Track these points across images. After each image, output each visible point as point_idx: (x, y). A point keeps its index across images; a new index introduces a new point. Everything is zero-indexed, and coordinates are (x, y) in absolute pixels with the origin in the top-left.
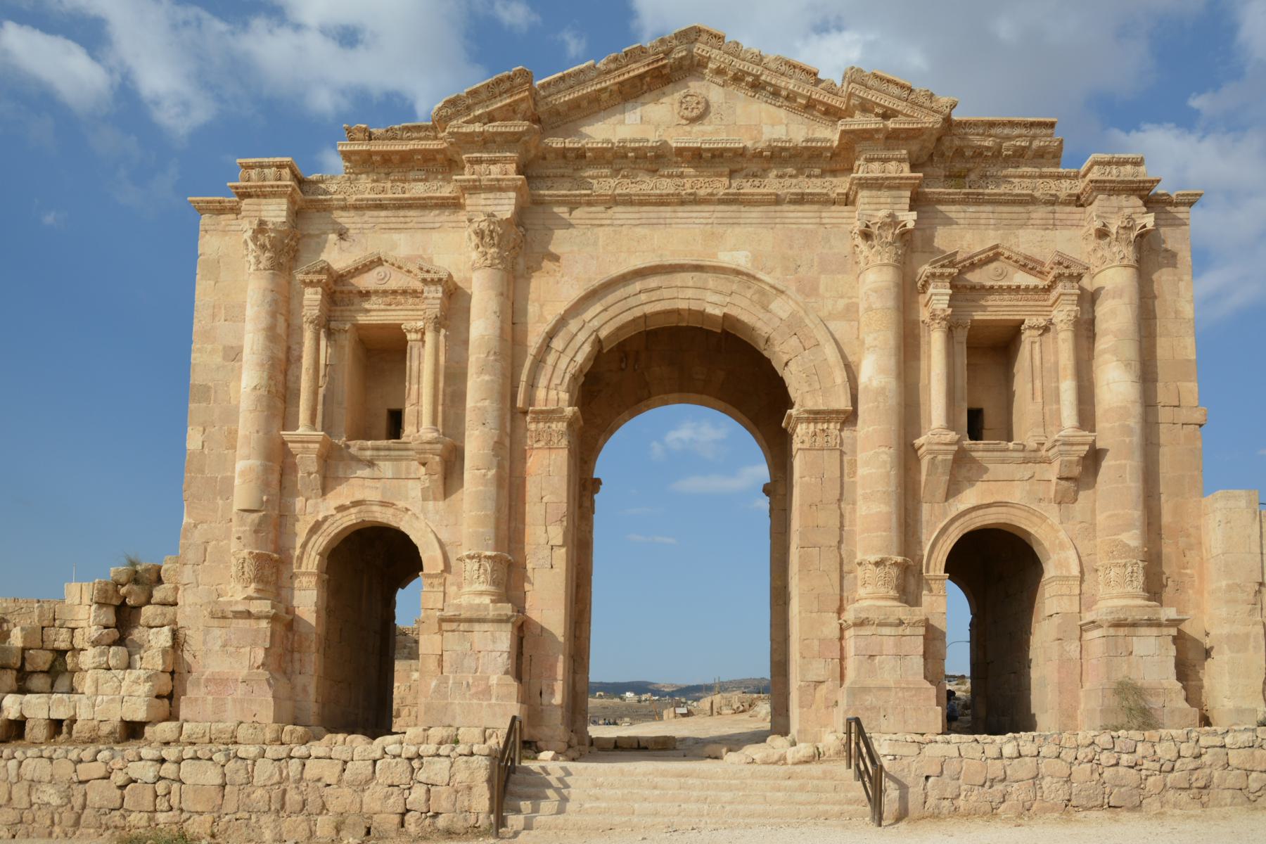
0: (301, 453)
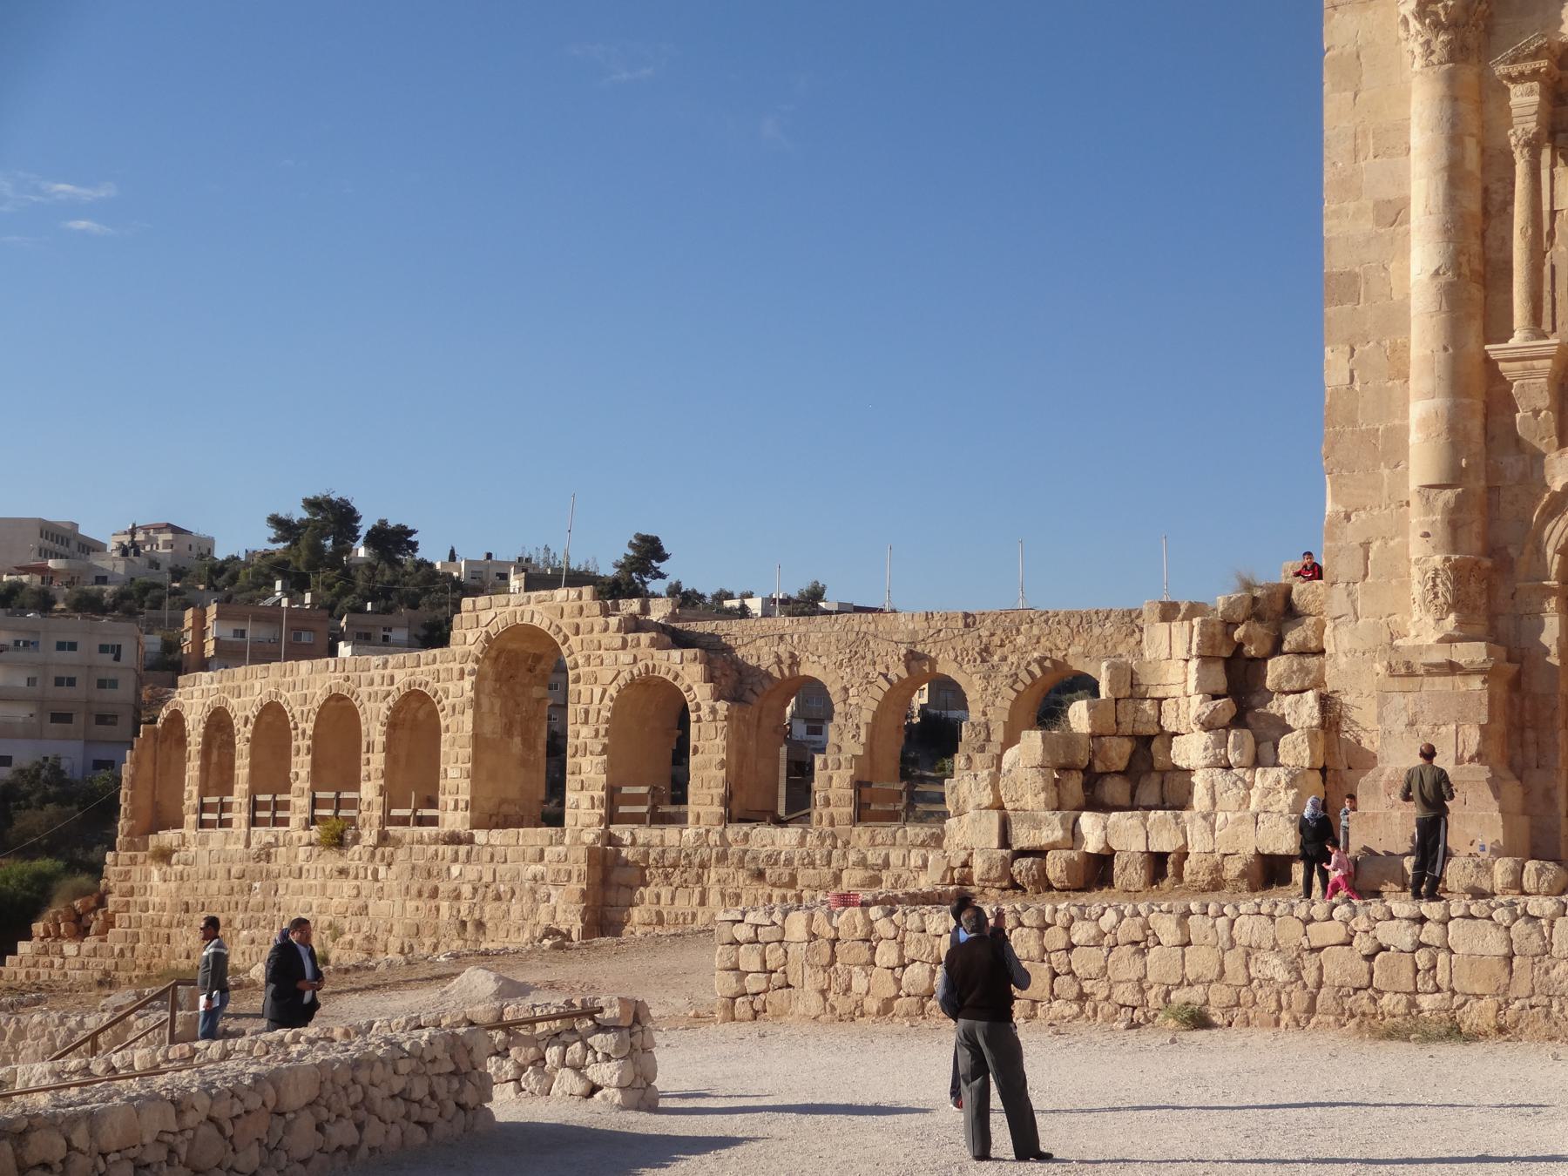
0: (1522, 377)
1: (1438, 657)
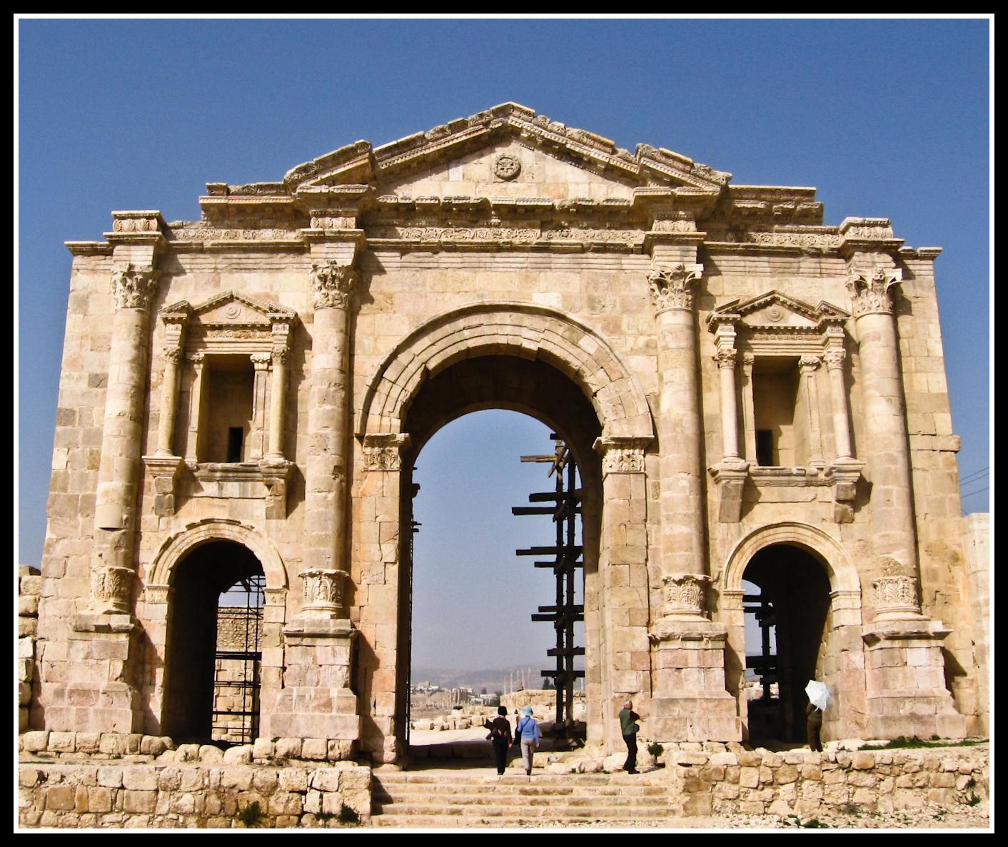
0: (159, 475)
1: (102, 622)
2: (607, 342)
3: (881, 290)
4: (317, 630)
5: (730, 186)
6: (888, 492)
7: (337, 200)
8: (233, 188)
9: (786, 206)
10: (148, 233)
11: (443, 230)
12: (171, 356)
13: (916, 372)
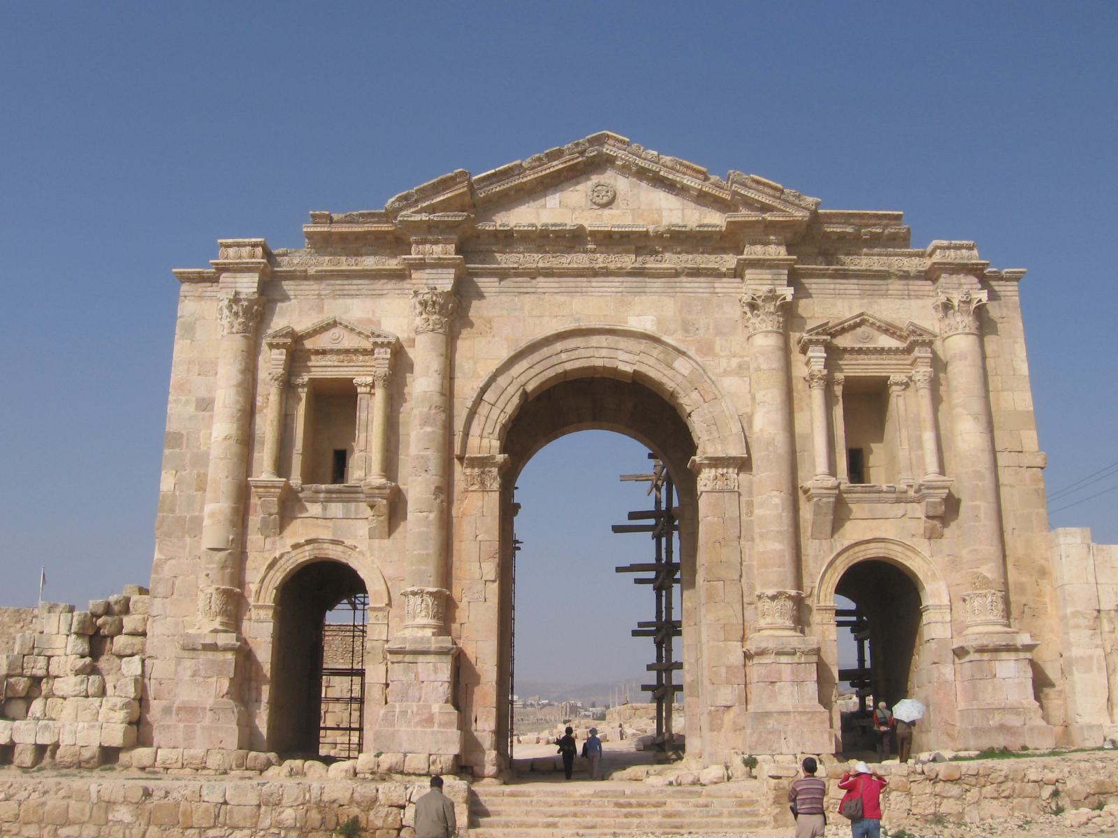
1: (208, 641)
2: (701, 363)
3: (967, 311)
4: (419, 647)
5: (820, 211)
6: (977, 507)
7: (438, 227)
8: (336, 217)
9: (874, 230)
10: (253, 260)
11: (540, 256)
12: (276, 380)
13: (1003, 391)
